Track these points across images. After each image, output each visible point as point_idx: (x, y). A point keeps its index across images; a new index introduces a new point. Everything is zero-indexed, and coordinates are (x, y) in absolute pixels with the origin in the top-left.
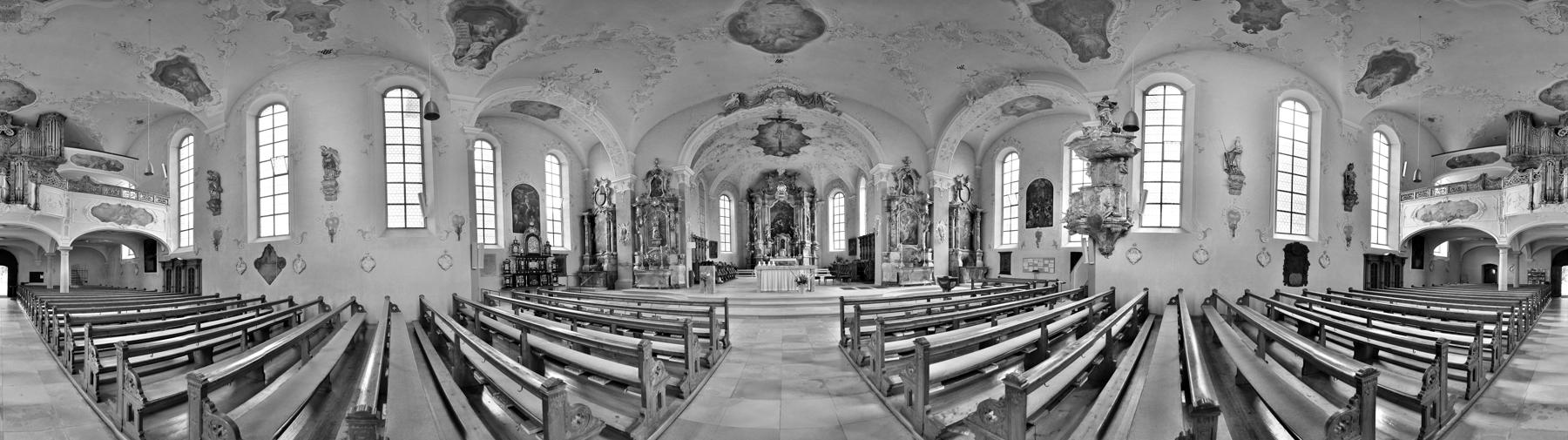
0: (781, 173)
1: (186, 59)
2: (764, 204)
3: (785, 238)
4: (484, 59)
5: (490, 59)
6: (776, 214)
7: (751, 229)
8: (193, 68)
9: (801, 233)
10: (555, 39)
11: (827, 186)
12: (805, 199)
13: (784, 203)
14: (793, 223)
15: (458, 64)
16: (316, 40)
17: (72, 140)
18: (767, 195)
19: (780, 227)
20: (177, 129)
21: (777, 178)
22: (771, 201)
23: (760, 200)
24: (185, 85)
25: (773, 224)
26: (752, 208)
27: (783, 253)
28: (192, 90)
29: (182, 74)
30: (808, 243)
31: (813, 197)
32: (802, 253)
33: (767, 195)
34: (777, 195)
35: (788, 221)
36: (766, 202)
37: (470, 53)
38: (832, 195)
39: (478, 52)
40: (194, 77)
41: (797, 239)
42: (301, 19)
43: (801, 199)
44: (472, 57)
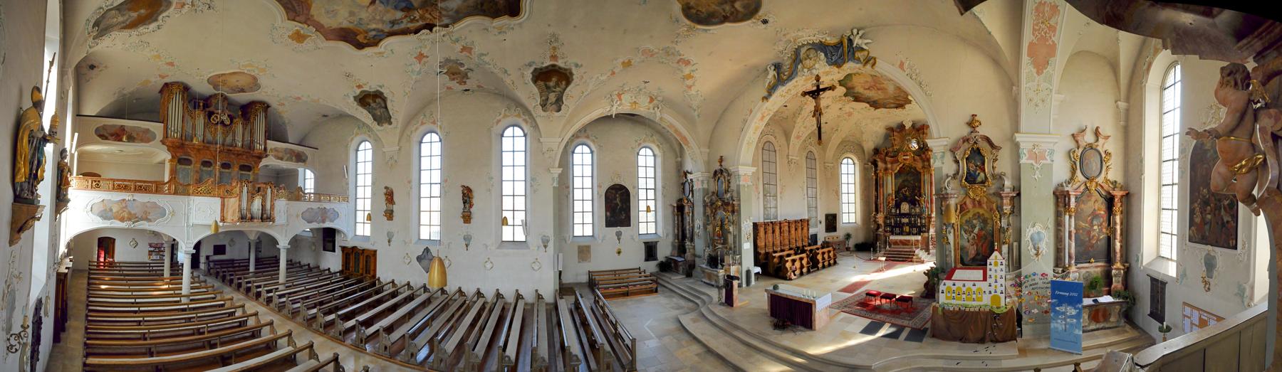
1: (382, 93)
4: (559, 103)
5: (563, 103)
8: (384, 100)
10: (598, 77)
15: (544, 111)
16: (461, 84)
17: (276, 133)
20: (357, 134)
24: (375, 109)
28: (379, 114)
29: (375, 102)
37: (549, 101)
39: (554, 100)
40: (383, 105)
42: (453, 75)
44: (552, 104)
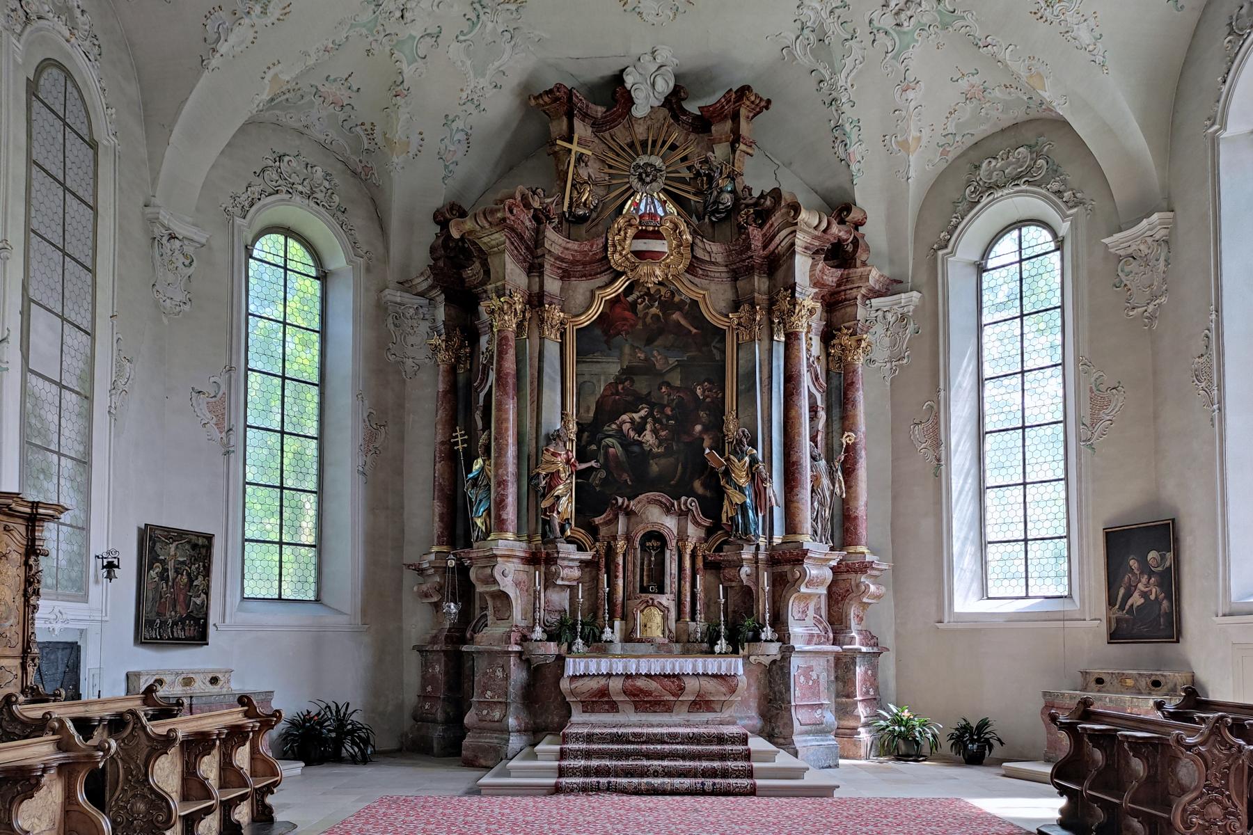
0: (646, 100)
2: (536, 300)
3: (670, 524)
6: (614, 369)
11: (941, 179)
14: (717, 425)
18: (554, 240)
19: (637, 457)
21: (621, 134)
22: (581, 288)
23: (514, 274)
25: (590, 433)
27: (654, 623)
32: (779, 621)
33: (554, 240)
35: (684, 417)
36: (552, 285)
38: (967, 247)
41: (746, 537)
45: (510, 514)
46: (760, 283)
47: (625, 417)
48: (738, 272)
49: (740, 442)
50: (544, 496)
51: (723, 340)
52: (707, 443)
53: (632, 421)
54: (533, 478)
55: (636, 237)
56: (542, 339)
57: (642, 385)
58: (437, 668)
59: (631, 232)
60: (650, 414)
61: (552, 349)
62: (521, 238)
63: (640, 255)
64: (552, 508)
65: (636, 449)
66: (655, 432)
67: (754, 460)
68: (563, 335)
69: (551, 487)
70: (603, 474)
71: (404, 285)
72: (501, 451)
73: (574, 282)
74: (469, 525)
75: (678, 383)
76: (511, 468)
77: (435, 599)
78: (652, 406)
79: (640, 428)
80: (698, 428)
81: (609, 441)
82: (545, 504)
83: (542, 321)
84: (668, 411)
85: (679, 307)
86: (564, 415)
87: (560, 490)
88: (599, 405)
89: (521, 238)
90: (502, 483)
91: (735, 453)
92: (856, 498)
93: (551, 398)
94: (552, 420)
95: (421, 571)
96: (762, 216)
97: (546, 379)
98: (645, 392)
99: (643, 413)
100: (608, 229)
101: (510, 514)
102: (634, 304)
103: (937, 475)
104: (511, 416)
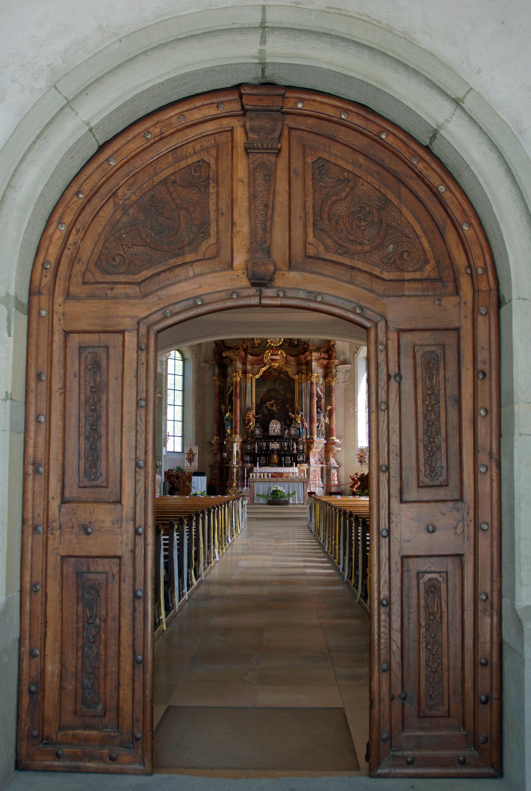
2: (245, 372)
6: (265, 390)
7: (221, 414)
9: (307, 425)
12: (314, 364)
13: (279, 371)
18: (250, 357)
22: (257, 367)
23: (239, 365)
25: (259, 407)
26: (223, 375)
30: (319, 442)
31: (330, 358)
34: (268, 356)
36: (249, 367)
43: (308, 363)
45: (238, 430)
46: (304, 367)
47: (268, 403)
48: (299, 364)
49: (298, 411)
50: (247, 425)
51: (294, 382)
52: (290, 410)
53: (270, 404)
54: (244, 420)
55: (272, 355)
56: (246, 382)
57: (273, 394)
58: (216, 471)
59: (270, 354)
60: (275, 402)
61: (249, 385)
62: (241, 357)
63: (272, 360)
64: (249, 428)
65: (271, 411)
66: (276, 407)
67: (302, 416)
68: (252, 381)
69: (249, 423)
70: (262, 418)
71: (205, 362)
72: (236, 414)
73: (255, 366)
74: (225, 431)
75: (282, 393)
76: (239, 418)
77: (216, 452)
78: (275, 400)
79: (272, 406)
80: (288, 406)
81: (264, 409)
82: (248, 427)
83: (246, 378)
84: (280, 401)
85: (283, 373)
86: (252, 403)
87: (251, 423)
88: (261, 399)
89: (241, 357)
90: (236, 422)
91: (297, 414)
92: (332, 424)
93: (248, 398)
94: (248, 404)
95: (211, 444)
96: (305, 350)
97: (247, 393)
98: (273, 396)
99: (273, 402)
100: (264, 353)
101: (238, 430)
102: (271, 372)
103: (355, 417)
104: (238, 404)
